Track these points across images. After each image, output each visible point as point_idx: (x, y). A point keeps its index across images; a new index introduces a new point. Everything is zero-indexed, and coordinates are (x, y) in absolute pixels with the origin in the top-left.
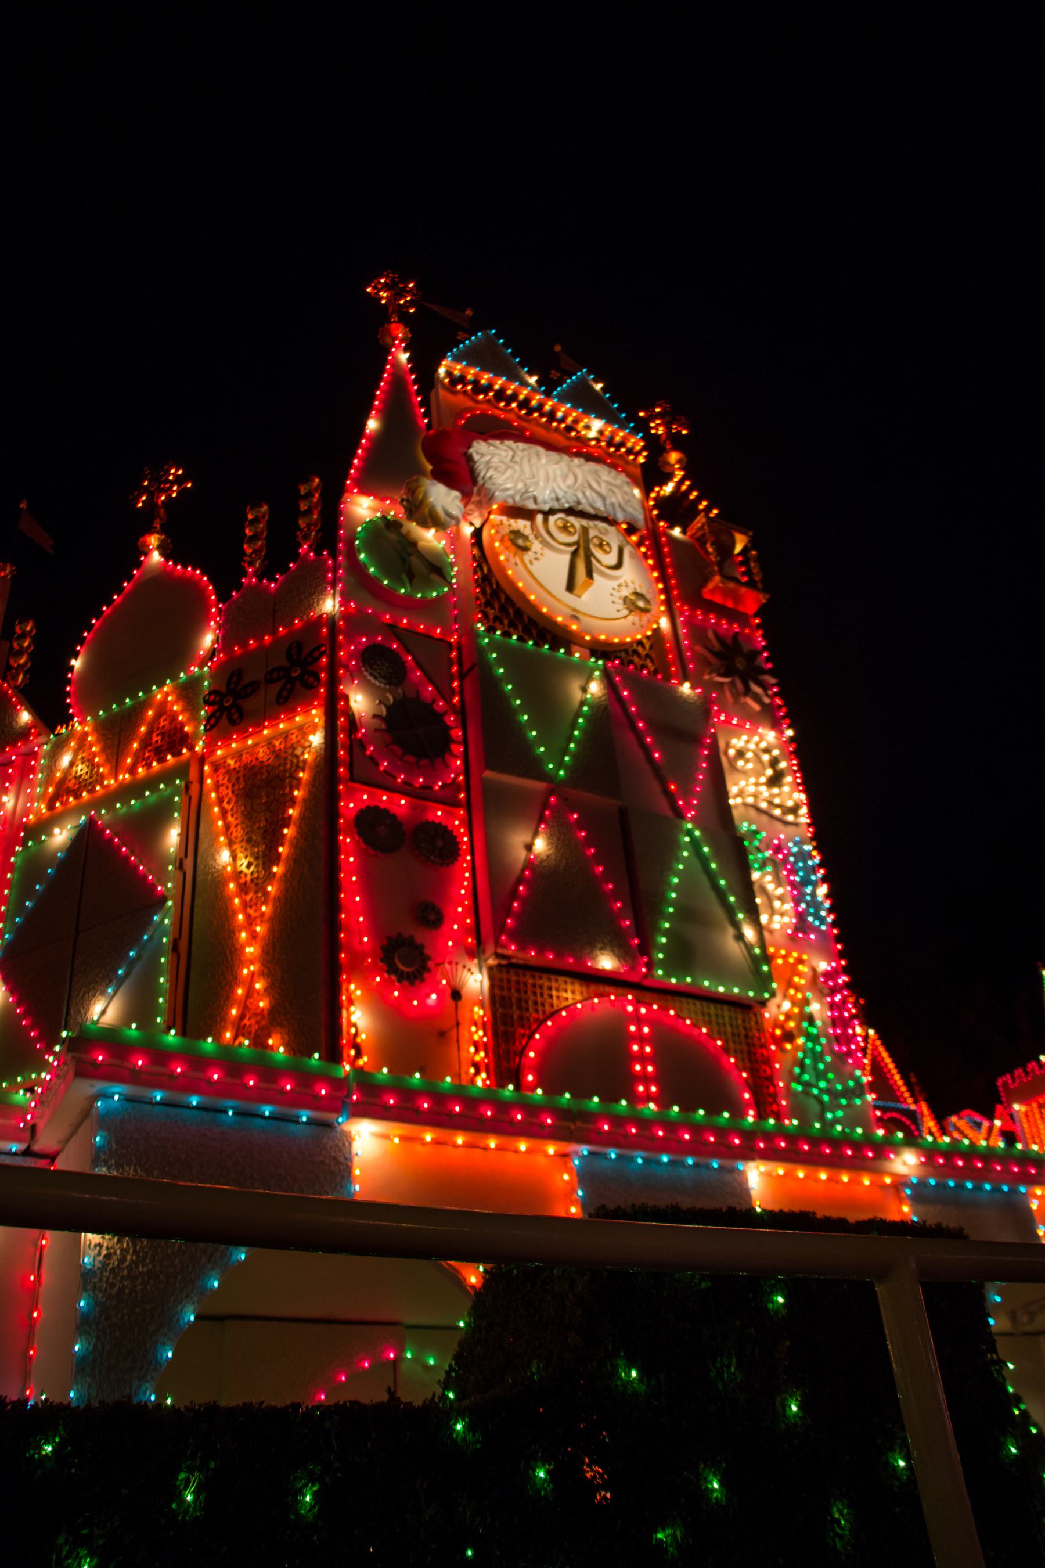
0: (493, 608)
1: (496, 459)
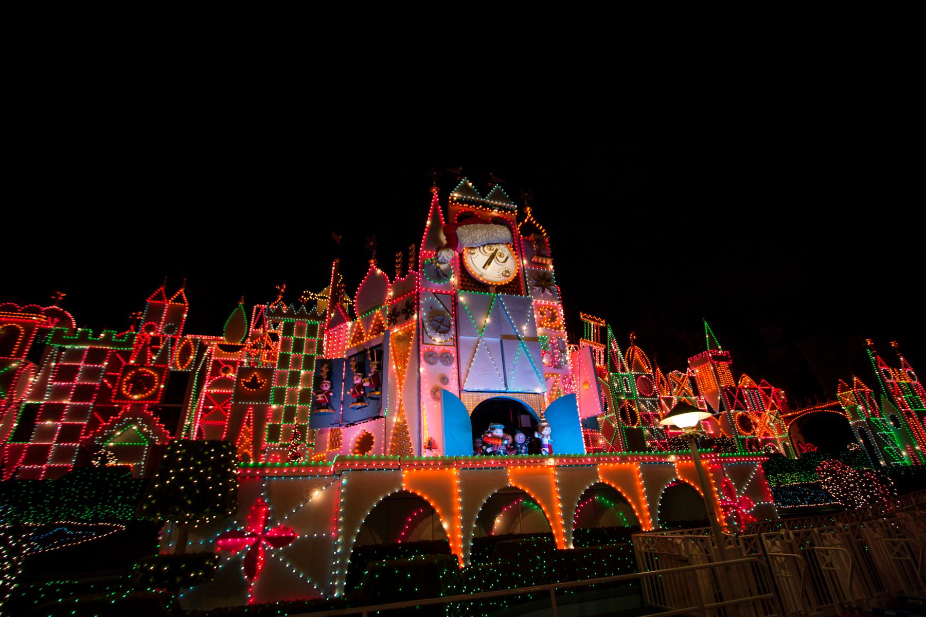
0: (466, 278)
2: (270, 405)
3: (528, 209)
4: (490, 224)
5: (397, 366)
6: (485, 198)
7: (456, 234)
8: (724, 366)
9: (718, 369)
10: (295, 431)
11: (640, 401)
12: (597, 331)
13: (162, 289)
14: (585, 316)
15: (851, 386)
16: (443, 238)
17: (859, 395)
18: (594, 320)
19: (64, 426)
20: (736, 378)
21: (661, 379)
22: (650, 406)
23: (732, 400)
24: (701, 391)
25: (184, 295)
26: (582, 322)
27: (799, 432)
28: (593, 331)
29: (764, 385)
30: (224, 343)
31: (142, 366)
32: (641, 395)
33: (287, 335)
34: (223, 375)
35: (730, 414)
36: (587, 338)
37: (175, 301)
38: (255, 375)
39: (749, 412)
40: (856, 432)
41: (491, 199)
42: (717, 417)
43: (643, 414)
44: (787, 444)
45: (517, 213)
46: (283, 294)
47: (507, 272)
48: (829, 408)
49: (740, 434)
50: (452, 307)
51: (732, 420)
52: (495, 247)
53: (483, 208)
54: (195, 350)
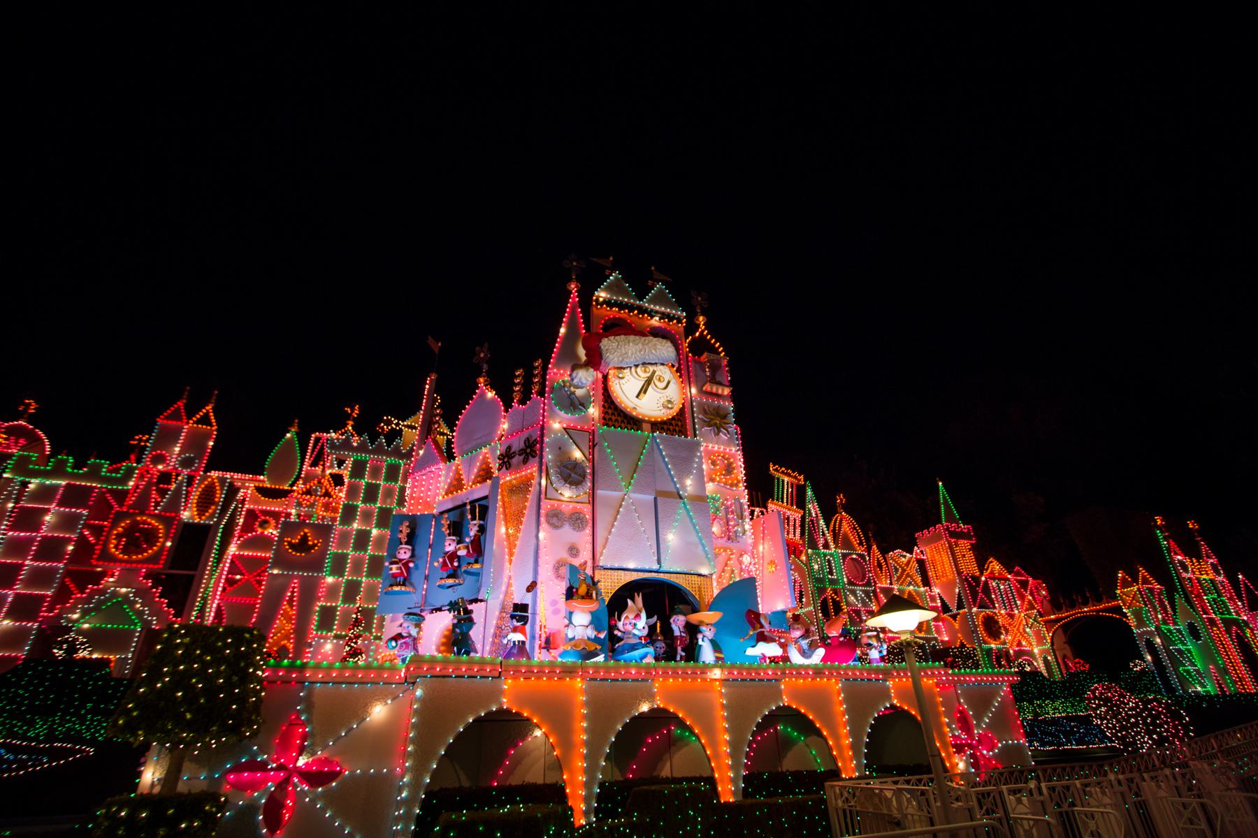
0: (611, 409)
1: (610, 348)
2: (324, 578)
3: (701, 318)
4: (646, 336)
5: (507, 529)
6: (643, 301)
7: (600, 348)
8: (964, 544)
9: (957, 549)
10: (357, 616)
11: (849, 590)
12: (792, 491)
13: (181, 404)
14: (777, 468)
15: (1135, 580)
16: (582, 352)
17: (1146, 594)
18: (789, 475)
19: (17, 596)
20: (981, 564)
21: (878, 561)
22: (862, 598)
23: (974, 594)
24: (933, 579)
25: (212, 414)
26: (772, 477)
27: (1065, 643)
28: (787, 490)
29: (1018, 574)
30: (265, 486)
31: (142, 513)
32: (850, 583)
33: (356, 478)
34: (260, 530)
35: (971, 613)
36: (778, 500)
37: (197, 422)
38: (306, 534)
39: (997, 611)
40: (1142, 645)
41: (650, 302)
42: (954, 617)
43: (852, 610)
44: (1049, 658)
45: (685, 322)
46: (354, 419)
47: (669, 402)
48: (1103, 610)
49: (985, 642)
50: (590, 449)
51: (974, 622)
52: (651, 368)
53: (639, 313)
54: (221, 493)
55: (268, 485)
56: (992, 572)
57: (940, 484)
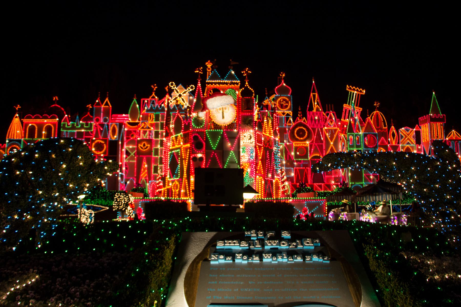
20: (447, 133)
26: (348, 92)
36: (349, 104)
37: (105, 105)
55: (131, 121)
56: (451, 137)
57: (434, 93)
